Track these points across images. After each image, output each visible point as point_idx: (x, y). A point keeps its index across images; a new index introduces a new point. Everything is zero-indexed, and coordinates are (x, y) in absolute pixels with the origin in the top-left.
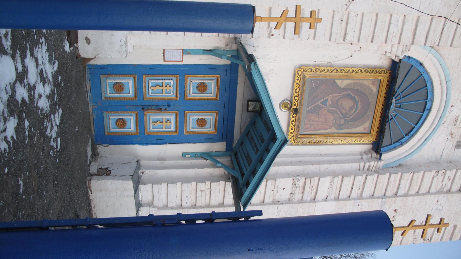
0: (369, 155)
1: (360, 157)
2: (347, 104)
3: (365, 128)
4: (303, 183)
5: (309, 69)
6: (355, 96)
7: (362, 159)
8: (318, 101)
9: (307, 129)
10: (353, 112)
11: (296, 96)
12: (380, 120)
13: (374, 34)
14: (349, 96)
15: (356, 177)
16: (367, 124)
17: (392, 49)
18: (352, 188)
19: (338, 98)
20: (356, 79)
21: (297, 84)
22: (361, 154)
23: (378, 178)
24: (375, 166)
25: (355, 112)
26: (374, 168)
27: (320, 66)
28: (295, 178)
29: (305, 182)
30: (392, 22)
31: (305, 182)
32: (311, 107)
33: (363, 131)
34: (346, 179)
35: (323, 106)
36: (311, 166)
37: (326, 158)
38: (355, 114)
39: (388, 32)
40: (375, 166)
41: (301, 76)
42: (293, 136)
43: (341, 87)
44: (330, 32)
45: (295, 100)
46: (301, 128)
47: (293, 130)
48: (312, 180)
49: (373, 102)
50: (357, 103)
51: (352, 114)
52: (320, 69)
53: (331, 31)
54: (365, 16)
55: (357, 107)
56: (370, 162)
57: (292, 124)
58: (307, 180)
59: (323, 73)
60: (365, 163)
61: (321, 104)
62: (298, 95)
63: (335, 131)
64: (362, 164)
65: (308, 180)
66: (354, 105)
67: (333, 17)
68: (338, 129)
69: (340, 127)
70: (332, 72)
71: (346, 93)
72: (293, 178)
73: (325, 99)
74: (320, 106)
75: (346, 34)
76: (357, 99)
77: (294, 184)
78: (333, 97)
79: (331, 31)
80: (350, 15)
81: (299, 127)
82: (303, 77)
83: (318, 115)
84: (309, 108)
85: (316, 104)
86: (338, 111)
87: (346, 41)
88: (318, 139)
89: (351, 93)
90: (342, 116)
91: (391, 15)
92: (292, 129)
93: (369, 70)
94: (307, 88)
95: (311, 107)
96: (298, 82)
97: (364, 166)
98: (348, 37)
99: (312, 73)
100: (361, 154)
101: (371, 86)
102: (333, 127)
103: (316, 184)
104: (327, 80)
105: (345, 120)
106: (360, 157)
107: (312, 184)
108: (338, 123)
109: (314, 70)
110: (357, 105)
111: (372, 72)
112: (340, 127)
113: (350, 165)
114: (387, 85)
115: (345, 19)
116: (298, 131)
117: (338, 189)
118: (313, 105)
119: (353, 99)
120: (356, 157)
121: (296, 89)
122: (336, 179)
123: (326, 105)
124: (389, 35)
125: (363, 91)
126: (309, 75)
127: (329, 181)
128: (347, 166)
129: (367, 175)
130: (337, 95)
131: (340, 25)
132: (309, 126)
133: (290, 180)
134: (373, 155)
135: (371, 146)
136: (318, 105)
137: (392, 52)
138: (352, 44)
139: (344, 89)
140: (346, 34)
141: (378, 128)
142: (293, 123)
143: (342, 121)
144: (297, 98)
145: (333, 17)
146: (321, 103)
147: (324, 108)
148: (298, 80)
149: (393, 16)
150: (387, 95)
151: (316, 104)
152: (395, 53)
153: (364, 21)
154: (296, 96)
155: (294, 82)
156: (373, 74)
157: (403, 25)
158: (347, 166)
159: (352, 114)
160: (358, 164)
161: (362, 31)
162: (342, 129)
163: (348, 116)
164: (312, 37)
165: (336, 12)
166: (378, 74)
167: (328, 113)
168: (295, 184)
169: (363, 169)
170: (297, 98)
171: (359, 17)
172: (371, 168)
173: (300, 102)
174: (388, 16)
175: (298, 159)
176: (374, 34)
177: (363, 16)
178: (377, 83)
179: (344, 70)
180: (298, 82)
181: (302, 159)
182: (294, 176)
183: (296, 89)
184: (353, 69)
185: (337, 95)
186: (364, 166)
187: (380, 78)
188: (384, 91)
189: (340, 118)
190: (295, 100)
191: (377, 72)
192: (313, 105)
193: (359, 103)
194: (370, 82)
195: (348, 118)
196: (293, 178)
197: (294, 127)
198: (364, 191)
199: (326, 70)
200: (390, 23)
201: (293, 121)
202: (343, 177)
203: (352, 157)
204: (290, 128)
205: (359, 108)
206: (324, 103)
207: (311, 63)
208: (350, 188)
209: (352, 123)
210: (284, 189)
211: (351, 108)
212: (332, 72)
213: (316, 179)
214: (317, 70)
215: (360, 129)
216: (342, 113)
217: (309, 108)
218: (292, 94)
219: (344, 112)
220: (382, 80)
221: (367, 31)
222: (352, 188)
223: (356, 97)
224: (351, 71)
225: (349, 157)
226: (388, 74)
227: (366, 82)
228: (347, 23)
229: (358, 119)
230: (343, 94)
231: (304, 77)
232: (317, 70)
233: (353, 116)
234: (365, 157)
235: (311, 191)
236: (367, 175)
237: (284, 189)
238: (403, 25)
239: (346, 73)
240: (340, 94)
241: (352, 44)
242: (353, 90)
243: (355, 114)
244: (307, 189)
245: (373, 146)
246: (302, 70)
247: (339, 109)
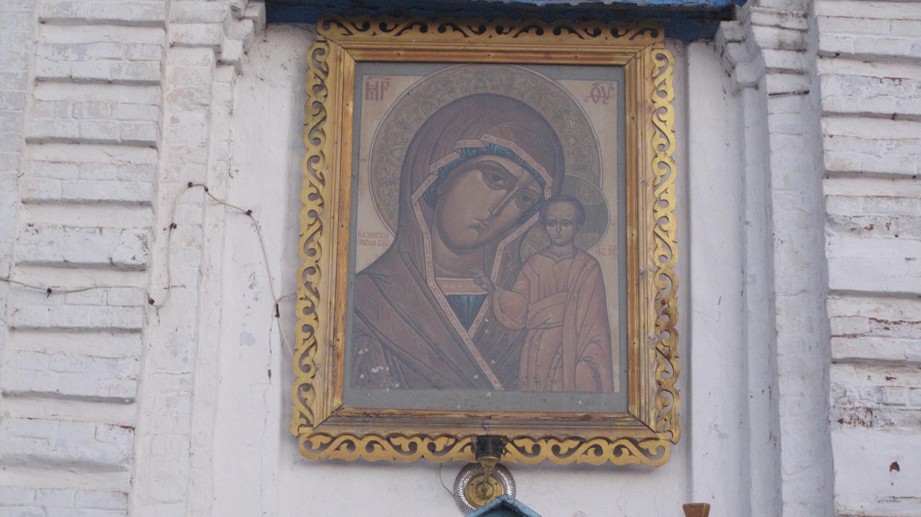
0: (733, 51)
1: (748, 93)
2: (474, 198)
3: (598, 96)
4: (865, 372)
5: (304, 401)
6: (434, 168)
7: (756, 87)
8: (459, 341)
9: (597, 376)
10: (512, 168)
11: (432, 447)
12: (557, 32)
13: (114, 143)
14: (434, 199)
15: (827, 106)
16: (577, 87)
17: (201, 46)
18: (894, 117)
19: (441, 245)
20: (355, 177)
21: (370, 446)
22: (737, 91)
23: (762, 25)
24: (775, 20)
25: (513, 157)
26: (792, 23)
27: (288, 347)
28: (836, 413)
29: (856, 362)
30: (65, 73)
31: (856, 362)
32: (488, 371)
33: (613, 102)
34: (837, 155)
35: (481, 314)
36: (782, 340)
37: (754, 268)
38: (524, 155)
39: (110, 83)
40: (775, 20)
41: (334, 432)
42: (634, 442)
43: (391, 239)
44: (106, 336)
45: (447, 449)
46: (591, 409)
47: (603, 443)
48: (837, 327)
49: (463, 82)
50: (469, 157)
51: (525, 166)
52: (302, 350)
53: (98, 330)
54: (35, 195)
55: (490, 150)
56: (759, 49)
57: (571, 451)
58: (838, 356)
59: (319, 335)
60: (768, 70)
61: (475, 326)
62: (422, 437)
63: (610, 238)
64: (774, 83)
65: (841, 349)
66: (479, 167)
67: (37, 329)
68: (600, 229)
69: (589, 219)
70: (317, 294)
71: (419, 213)
72: (835, 424)
73: (447, 308)
74: (484, 326)
75: (113, 266)
76: (454, 157)
77: (867, 417)
78: (437, 274)
79: (98, 330)
80: (31, 258)
81: (587, 418)
82: (336, 424)
83: (525, 330)
84: (493, 378)
85: (472, 347)
86: (509, 239)
87: (141, 260)
88: (651, 314)
89: (423, 188)
90: (536, 217)
91: (39, 80)
92: (598, 450)
93: (312, 124)
94: (389, 397)
95: (488, 371)
96: (361, 445)
97: (782, 71)
98: (123, 256)
99: (317, 383)
100: (737, 91)
101: (389, 102)
102: (593, 252)
103: (867, 307)
104: (357, 312)
105: (557, 197)
106: (748, 93)
107: (866, 327)
108: (567, 230)
109: (305, 378)
110: (479, 152)
111: (321, 108)
112: (589, 219)
113: (776, 141)
114: (383, 28)
115: (50, 278)
116: (608, 422)
117: (903, 187)
118: (479, 359)
119: (448, 177)
120: (750, 116)
121: (398, 448)
122: (836, 209)
123: (480, 299)
124: (123, 76)
125: (411, 136)
126: (326, 395)
127: (850, 240)
128: (786, 158)
129: (822, 55)
130: (429, 255)
131: (71, 298)
132: (582, 366)
133: (845, 440)
134: (728, 36)
135: (697, 54)
136: (477, 340)
137: (211, 40)
138: (173, 226)
139: (403, 228)
140: (113, 266)
141: (597, 33)
142: (564, 447)
143: (563, 210)
144: (440, 444)
145: (37, 329)
146: (467, 326)
147: (491, 308)
148: (351, 445)
149: (43, 75)
150: (434, 20)
151: (472, 347)
152: (215, 28)
153: (56, 195)
154: (432, 447)
155: (361, 463)
156: (328, 105)
157: (83, 21)
158: (786, 158)
159: (525, 166)
160: (775, 105)
161: (103, 195)
162: (602, 208)
163: (535, 188)
164: (125, 414)
165: (17, 322)
166: (329, 82)
167: (520, 285)
168: (869, 410)
169: (800, 73)
170: (440, 444)
171: (44, 216)
172: (791, 37)
173: (459, 424)
174: (47, 92)
175: (757, 407)
176: (114, 143)
177: (40, 202)
178: (373, 78)
179: (311, 238)
180: (361, 445)
181: (755, 384)
182: (827, 416)
183: (398, 448)
184: (305, 199)
185: (429, 255)
186: (782, 71)
187: (349, 63)
188: (413, 37)
189: (544, 222)
190: (447, 449)
191: (322, 86)
192: (479, 359)
193: (469, 143)
194: (368, 107)
195: (542, 185)
196: (835, 424)
197: (582, 441)
198: (907, 52)
199: (309, 319)
200: (72, 80)
201: (556, 449)
202: (828, 175)
203: (750, 135)
204: (592, 458)
205: (493, 139)
206: (465, 309)
207: (274, 392)
208: (898, 124)
209: (569, 161)
210: (895, 466)
211: (496, 177)
212: (317, 294)
213: (836, 306)
214: (307, 361)
215: (602, 119)
216: (521, 220)
217: (493, 378)
218: (422, 463)
219: (513, 210)
220: (359, 55)
221: (101, 174)
222: (894, 117)
223: (443, 162)
224: (313, 205)
225: (751, 152)
226: (335, 32)
227: (371, 129)
228: (66, 265)
229: (549, 139)
230: (424, 227)
231: (336, 417)
232: (307, 361)
233: (535, 165)
234: (743, 74)
235: (905, 329)
236: (822, 55)
237: (895, 466)
238: (83, 21)
239: (321, 229)
240: (427, 241)
241: (173, 226)
242: (407, 181)
243: (524, 155)
244: (891, 347)
245: (691, 41)
246: (307, 431)
247: (502, 234)
